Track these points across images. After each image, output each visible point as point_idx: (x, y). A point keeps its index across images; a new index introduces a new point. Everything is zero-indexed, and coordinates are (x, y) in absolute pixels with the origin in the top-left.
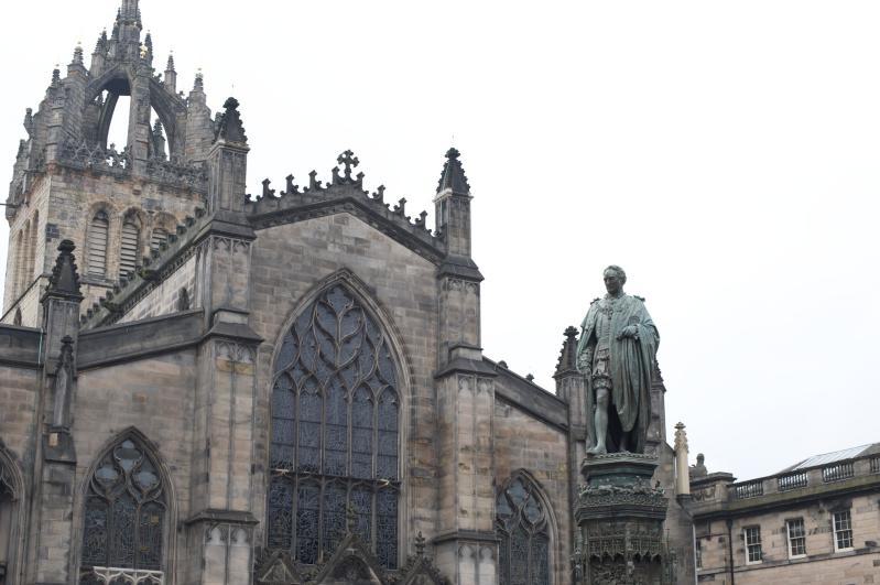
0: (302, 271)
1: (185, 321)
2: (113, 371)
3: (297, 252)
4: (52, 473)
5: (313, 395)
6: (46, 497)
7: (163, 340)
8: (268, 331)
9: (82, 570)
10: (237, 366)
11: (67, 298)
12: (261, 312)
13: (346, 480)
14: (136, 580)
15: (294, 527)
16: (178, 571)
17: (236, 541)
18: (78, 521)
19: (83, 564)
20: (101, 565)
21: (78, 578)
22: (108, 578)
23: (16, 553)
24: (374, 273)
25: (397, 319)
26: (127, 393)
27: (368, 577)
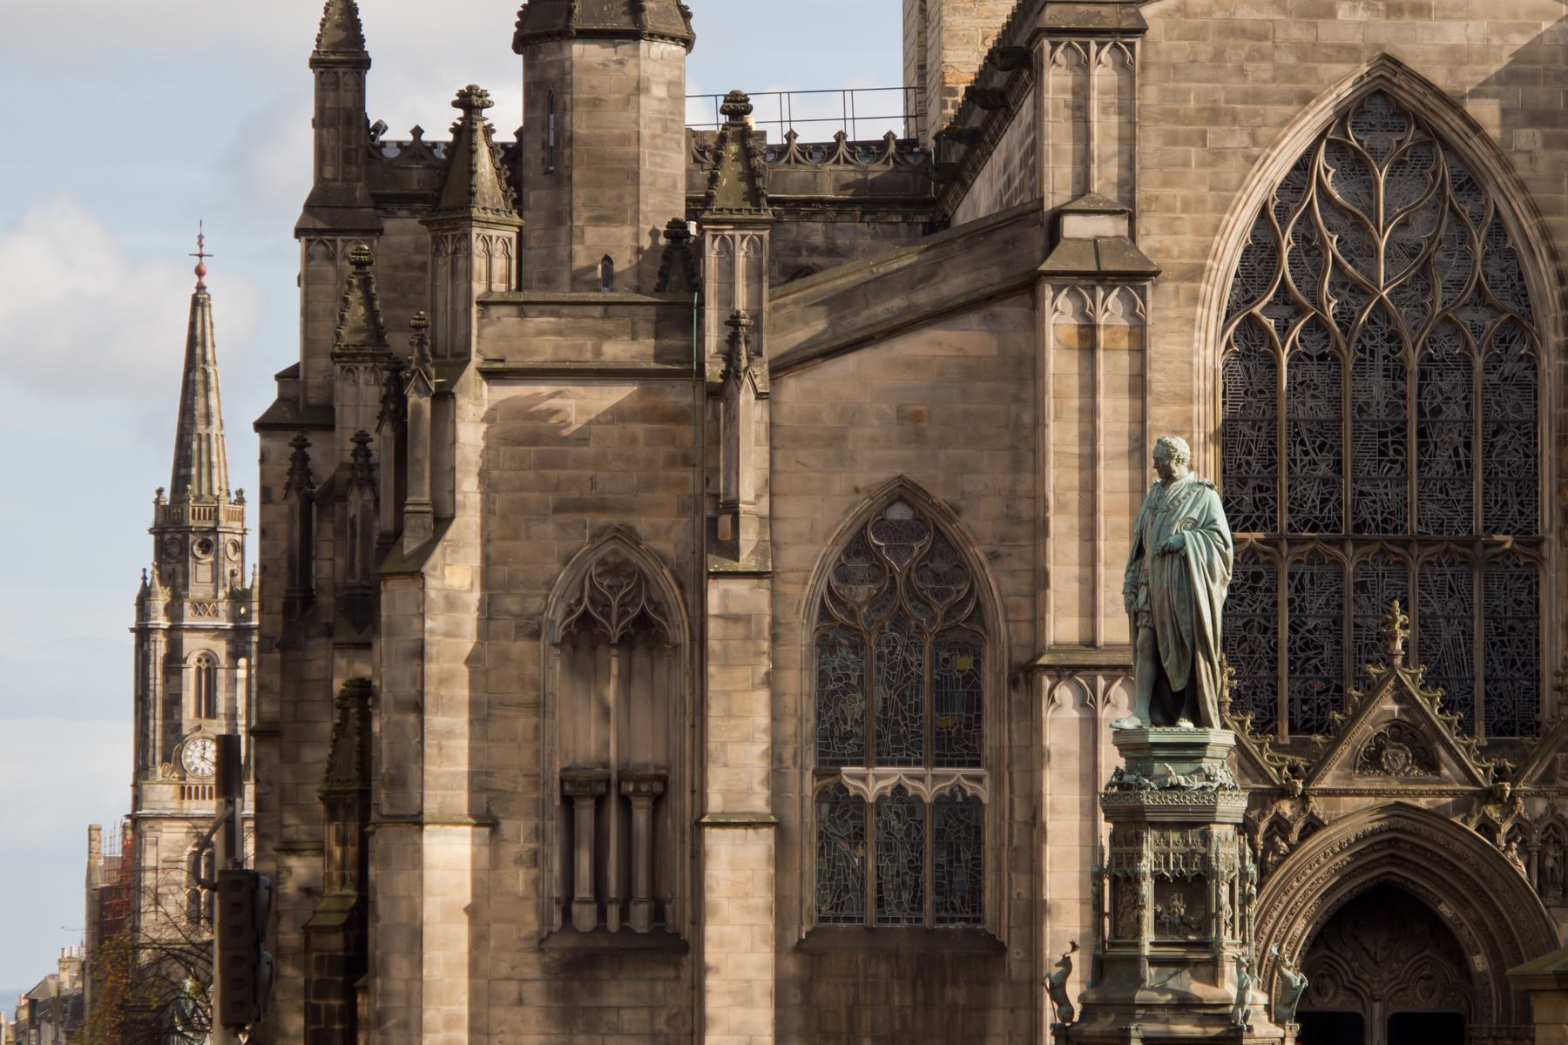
0: (1274, 79)
1: (999, 236)
2: (851, 361)
3: (1262, 37)
4: (725, 595)
5: (1322, 357)
6: (713, 644)
7: (955, 284)
8: (1197, 230)
9: (818, 774)
10: (1102, 336)
11: (739, 225)
12: (1179, 192)
13: (1406, 544)
14: (928, 793)
15: (1284, 656)
16: (1016, 768)
17: (1115, 706)
18: (798, 682)
19: (821, 763)
20: (854, 764)
21: (808, 791)
22: (871, 792)
23: (682, 748)
24: (1456, 57)
25: (1519, 161)
26: (885, 407)
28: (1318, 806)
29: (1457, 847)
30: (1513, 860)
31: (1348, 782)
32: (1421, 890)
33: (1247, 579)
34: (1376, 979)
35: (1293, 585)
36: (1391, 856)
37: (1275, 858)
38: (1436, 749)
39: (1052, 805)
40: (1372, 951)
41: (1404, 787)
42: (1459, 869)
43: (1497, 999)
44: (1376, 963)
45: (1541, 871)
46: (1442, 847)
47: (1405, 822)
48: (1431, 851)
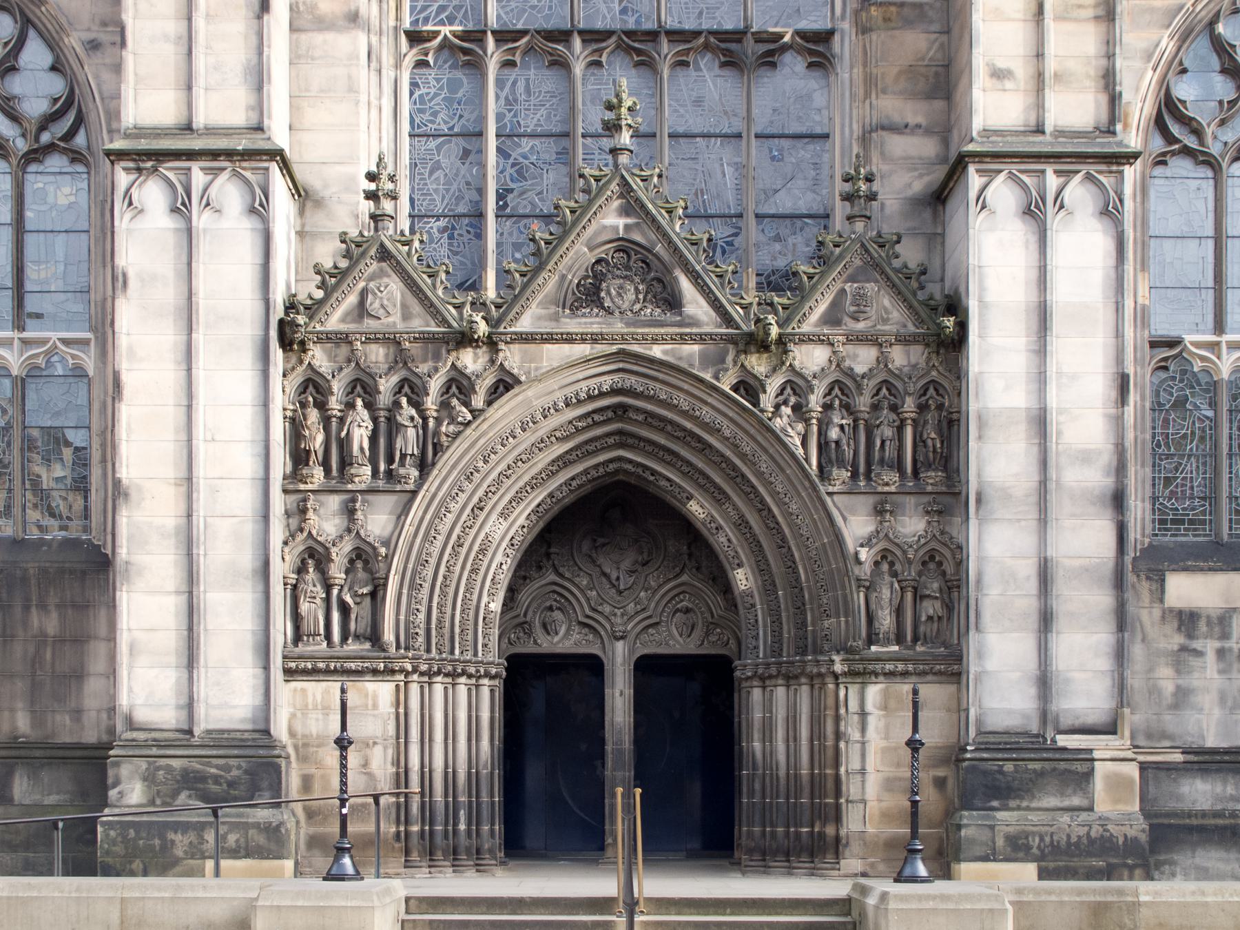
27: (673, 302)
28: (512, 357)
29: (706, 413)
30: (783, 430)
31: (553, 324)
32: (663, 483)
33: (441, 89)
34: (619, 612)
35: (503, 95)
36: (620, 432)
37: (452, 428)
38: (676, 279)
39: (130, 349)
40: (614, 576)
41: (632, 330)
42: (710, 446)
43: (765, 626)
44: (620, 593)
45: (823, 446)
46: (685, 414)
47: (633, 379)
48: (671, 422)
